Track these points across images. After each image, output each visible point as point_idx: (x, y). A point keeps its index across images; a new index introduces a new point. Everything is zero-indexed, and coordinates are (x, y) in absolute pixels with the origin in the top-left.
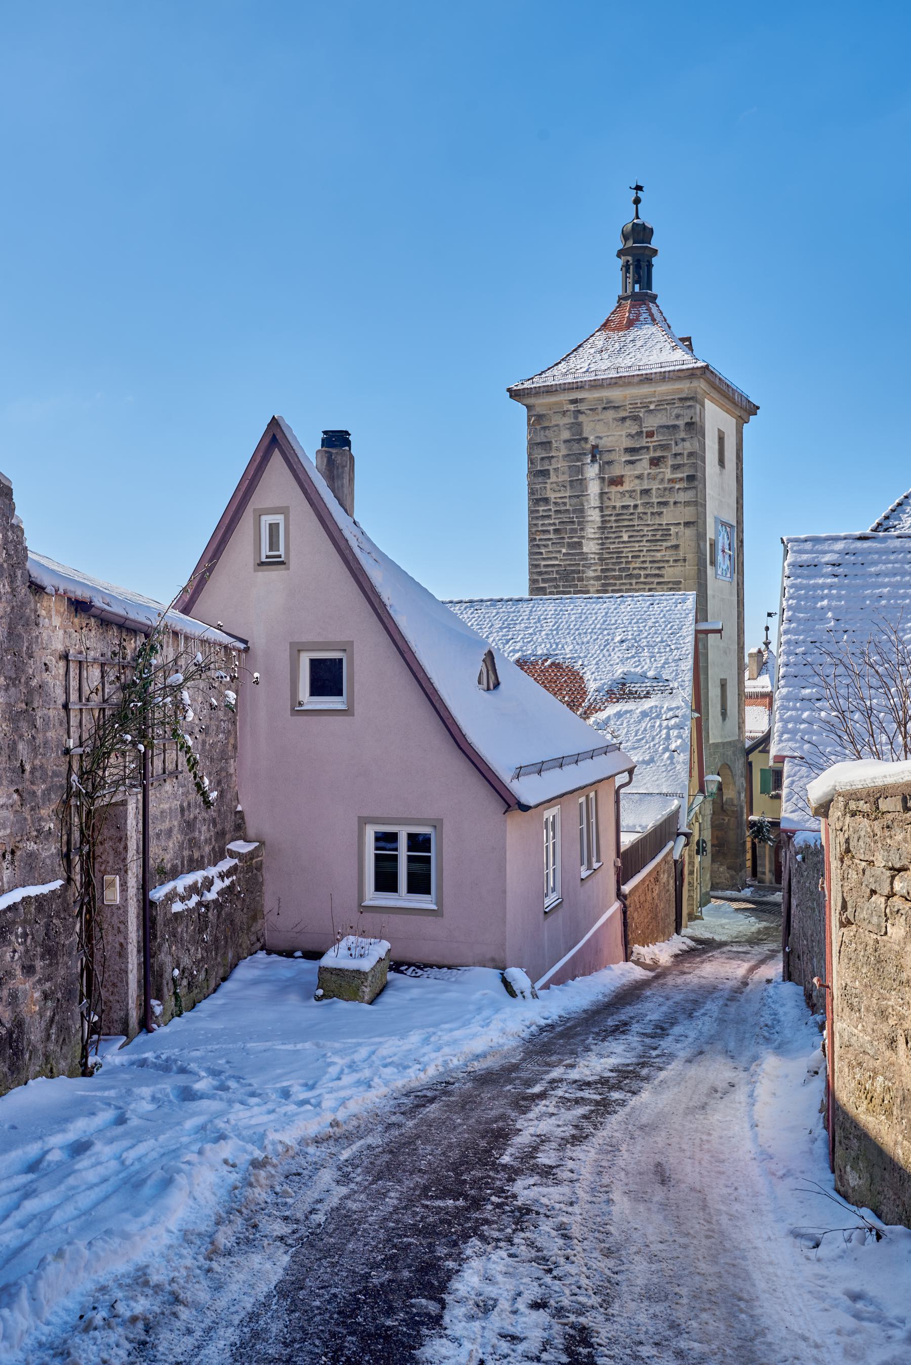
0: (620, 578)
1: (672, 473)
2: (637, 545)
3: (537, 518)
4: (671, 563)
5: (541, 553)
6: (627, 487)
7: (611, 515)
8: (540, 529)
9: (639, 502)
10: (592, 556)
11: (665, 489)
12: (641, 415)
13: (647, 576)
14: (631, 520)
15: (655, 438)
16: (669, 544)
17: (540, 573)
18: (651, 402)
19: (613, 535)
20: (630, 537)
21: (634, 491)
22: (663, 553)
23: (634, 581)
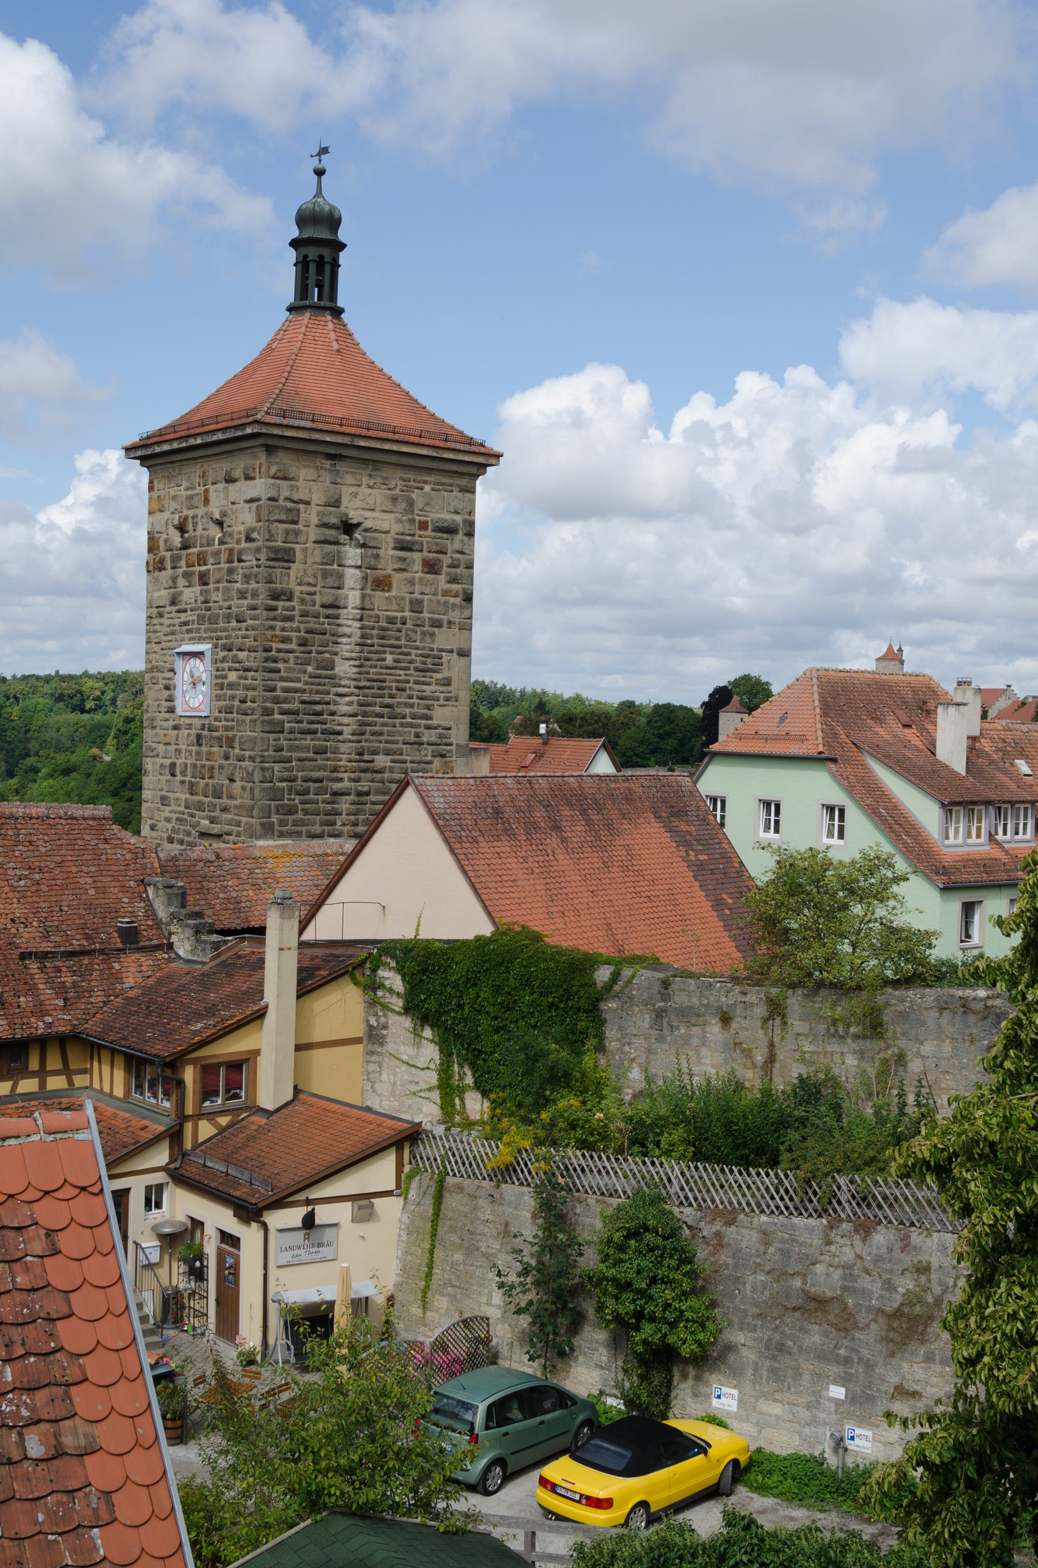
0: (380, 716)
1: (449, 582)
2: (402, 672)
3: (275, 619)
4: (442, 702)
5: (279, 671)
6: (393, 593)
7: (373, 628)
8: (278, 633)
9: (407, 614)
10: (347, 682)
11: (438, 602)
12: (414, 496)
13: (414, 717)
14: (398, 639)
15: (429, 533)
16: (440, 676)
17: (276, 700)
18: (426, 482)
19: (375, 656)
20: (396, 661)
21: (403, 598)
22: (433, 688)
23: (398, 721)
